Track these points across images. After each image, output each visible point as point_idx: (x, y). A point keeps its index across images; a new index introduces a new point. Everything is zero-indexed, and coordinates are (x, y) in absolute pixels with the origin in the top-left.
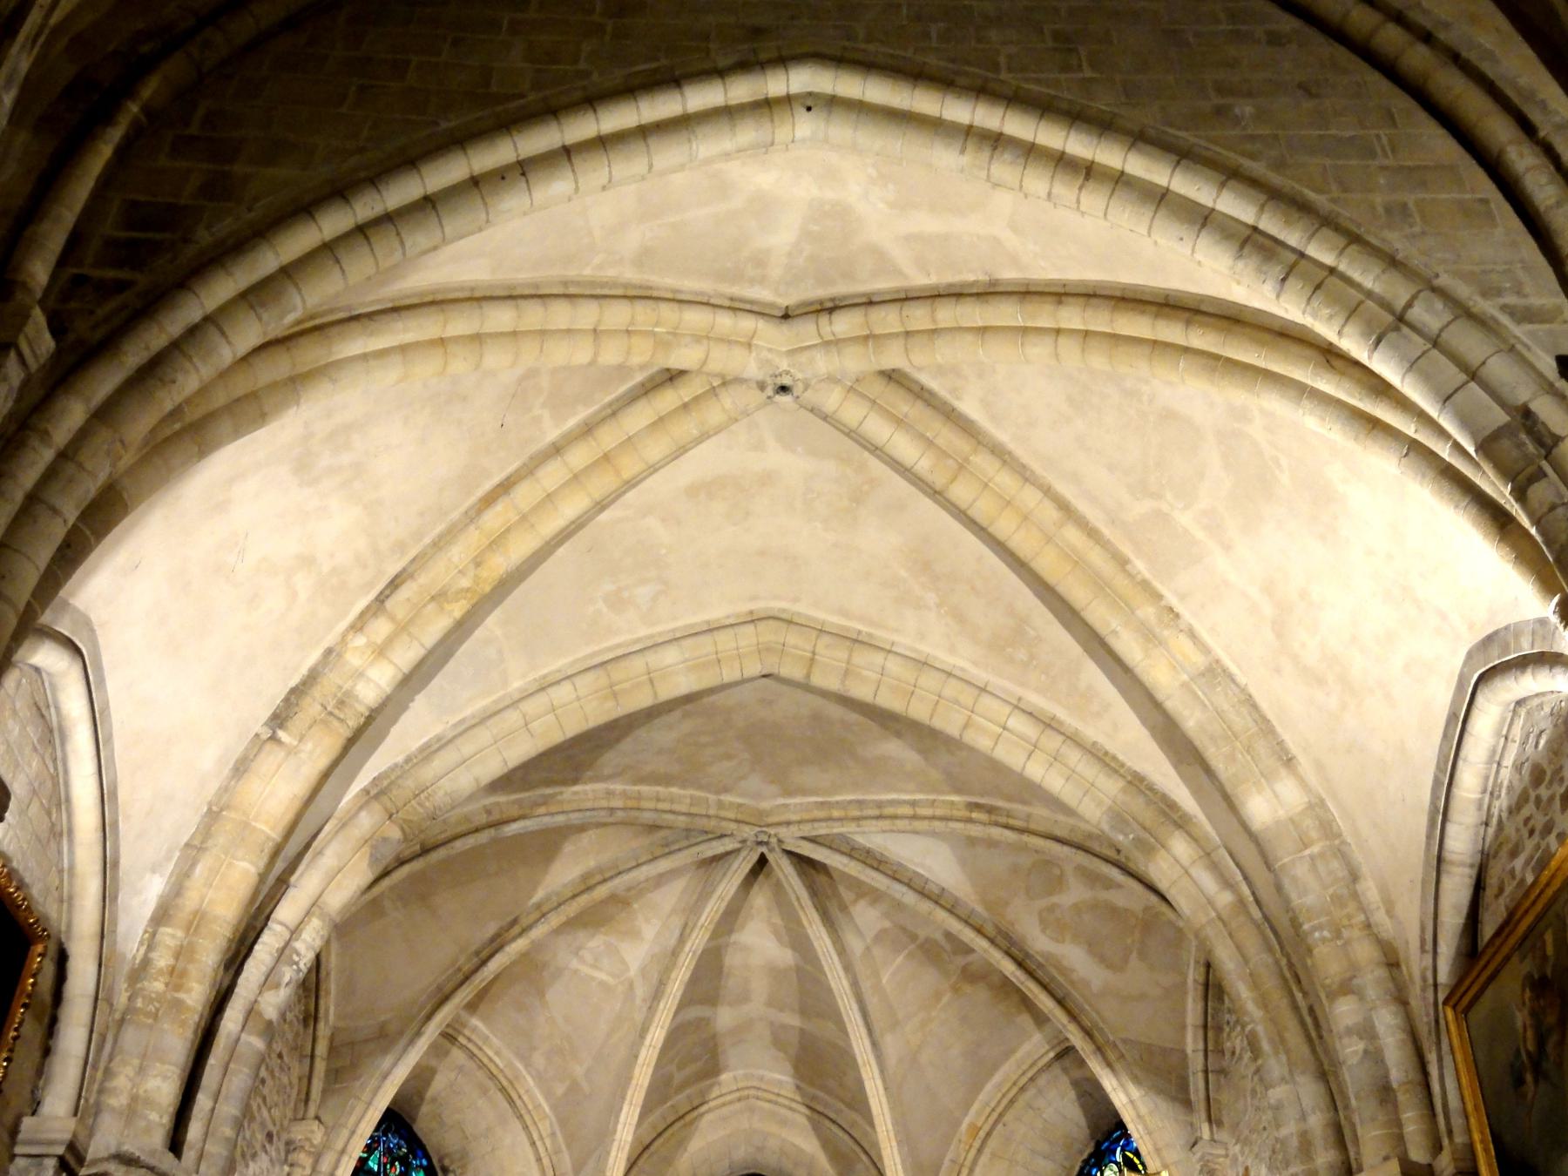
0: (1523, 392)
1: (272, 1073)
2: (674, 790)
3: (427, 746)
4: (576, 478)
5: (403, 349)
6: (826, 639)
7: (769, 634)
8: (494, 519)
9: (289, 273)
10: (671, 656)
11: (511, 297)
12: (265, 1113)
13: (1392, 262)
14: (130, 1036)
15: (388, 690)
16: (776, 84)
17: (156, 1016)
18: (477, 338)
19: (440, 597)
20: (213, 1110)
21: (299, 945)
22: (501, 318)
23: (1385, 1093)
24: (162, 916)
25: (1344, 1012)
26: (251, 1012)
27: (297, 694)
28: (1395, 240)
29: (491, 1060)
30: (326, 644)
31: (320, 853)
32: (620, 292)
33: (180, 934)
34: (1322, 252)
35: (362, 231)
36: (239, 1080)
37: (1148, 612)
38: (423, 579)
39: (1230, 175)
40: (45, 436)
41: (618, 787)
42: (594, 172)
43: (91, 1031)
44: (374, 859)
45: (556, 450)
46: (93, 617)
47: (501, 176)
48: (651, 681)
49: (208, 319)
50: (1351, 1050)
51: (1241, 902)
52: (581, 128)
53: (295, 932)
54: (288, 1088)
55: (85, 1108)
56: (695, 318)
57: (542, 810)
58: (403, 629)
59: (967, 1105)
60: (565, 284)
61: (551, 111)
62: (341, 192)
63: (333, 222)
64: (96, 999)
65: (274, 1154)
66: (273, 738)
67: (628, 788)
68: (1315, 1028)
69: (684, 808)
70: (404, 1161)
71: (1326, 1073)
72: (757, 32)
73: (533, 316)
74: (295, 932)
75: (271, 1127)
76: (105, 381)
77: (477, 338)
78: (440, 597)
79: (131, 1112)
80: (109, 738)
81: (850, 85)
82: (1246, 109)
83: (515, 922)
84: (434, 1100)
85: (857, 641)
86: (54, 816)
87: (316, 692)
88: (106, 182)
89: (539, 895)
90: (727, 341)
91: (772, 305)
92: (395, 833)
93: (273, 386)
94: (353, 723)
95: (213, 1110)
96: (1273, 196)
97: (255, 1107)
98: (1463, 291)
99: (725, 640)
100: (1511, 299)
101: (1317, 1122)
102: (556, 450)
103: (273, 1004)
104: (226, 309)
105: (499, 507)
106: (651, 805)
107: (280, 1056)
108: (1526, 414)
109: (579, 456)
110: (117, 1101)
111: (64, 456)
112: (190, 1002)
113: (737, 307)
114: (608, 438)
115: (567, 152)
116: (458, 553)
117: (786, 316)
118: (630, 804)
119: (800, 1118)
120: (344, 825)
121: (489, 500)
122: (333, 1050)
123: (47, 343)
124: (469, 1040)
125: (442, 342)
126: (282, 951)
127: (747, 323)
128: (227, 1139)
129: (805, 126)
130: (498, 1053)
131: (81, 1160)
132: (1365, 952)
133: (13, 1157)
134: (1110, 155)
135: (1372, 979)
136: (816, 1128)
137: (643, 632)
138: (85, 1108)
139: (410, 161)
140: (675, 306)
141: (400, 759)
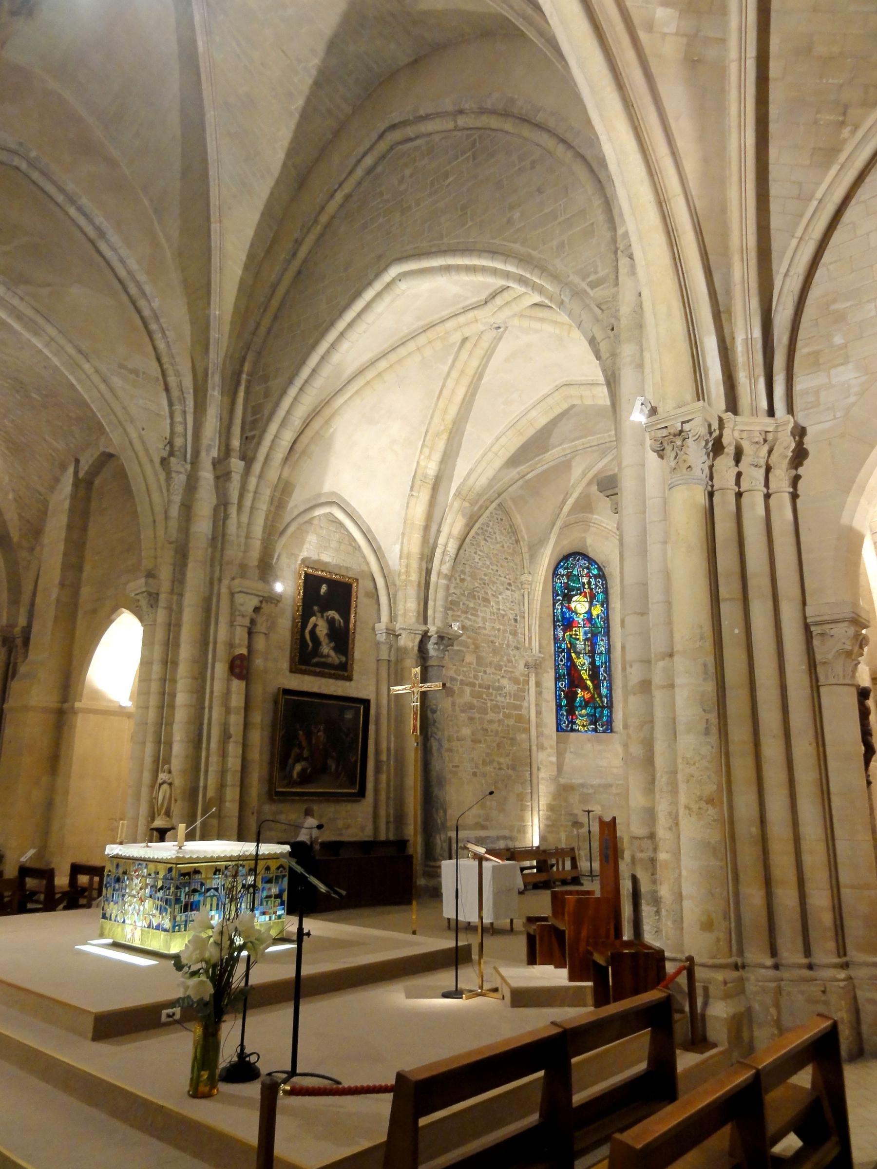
1: (502, 566)
2: (589, 438)
3: (468, 473)
4: (457, 381)
5: (357, 392)
6: (582, 387)
8: (441, 404)
9: (288, 412)
10: (533, 413)
11: (384, 355)
12: (503, 579)
13: (555, 277)
14: (400, 595)
15: (437, 469)
17: (406, 586)
18: (379, 375)
19: (438, 435)
20: (435, 605)
21: (448, 549)
22: (383, 365)
24: (401, 557)
26: (439, 573)
27: (414, 477)
28: (558, 265)
29: (605, 528)
30: (416, 461)
31: (446, 519)
32: (421, 331)
33: (406, 561)
35: (301, 389)
36: (441, 594)
38: (430, 431)
39: (506, 255)
40: (248, 491)
41: (565, 446)
42: (353, 335)
43: (389, 595)
44: (464, 516)
45: (448, 374)
46: (335, 491)
47: (328, 352)
48: (531, 424)
49: (276, 436)
52: (341, 325)
53: (446, 545)
54: (515, 567)
55: (392, 617)
56: (450, 324)
57: (539, 465)
58: (432, 449)
60: (401, 339)
61: (332, 324)
62: (290, 382)
63: (293, 391)
64: (387, 586)
65: (513, 588)
66: (412, 495)
67: (570, 445)
69: (595, 443)
70: (588, 568)
72: (380, 257)
73: (393, 357)
74: (446, 545)
75: (509, 581)
76: (257, 467)
77: (379, 375)
78: (438, 435)
79: (405, 615)
80: (360, 516)
82: (517, 215)
83: (567, 493)
84: (590, 546)
86: (354, 544)
87: (417, 477)
88: (246, 400)
89: (572, 482)
90: (467, 324)
91: (478, 301)
92: (467, 504)
93: (321, 428)
94: (431, 482)
95: (435, 605)
96: (523, 260)
97: (495, 580)
98: (575, 279)
99: (550, 400)
100: (592, 278)
102: (448, 374)
103: (446, 569)
104: (278, 431)
105: (441, 400)
106: (582, 447)
107: (506, 559)
109: (454, 374)
110: (400, 612)
111: (256, 492)
112: (413, 579)
113: (466, 310)
114: (459, 365)
115: (342, 334)
116: (436, 420)
117: (486, 302)
118: (573, 450)
120: (451, 506)
121: (438, 398)
122: (530, 549)
123: (242, 464)
124: (594, 523)
125: (368, 383)
126: (444, 552)
127: (471, 315)
128: (441, 612)
129: (403, 286)
130: (607, 524)
131: (394, 631)
133: (376, 635)
137: (523, 408)
138: (392, 617)
139: (303, 362)
140: (441, 325)
141: (462, 480)
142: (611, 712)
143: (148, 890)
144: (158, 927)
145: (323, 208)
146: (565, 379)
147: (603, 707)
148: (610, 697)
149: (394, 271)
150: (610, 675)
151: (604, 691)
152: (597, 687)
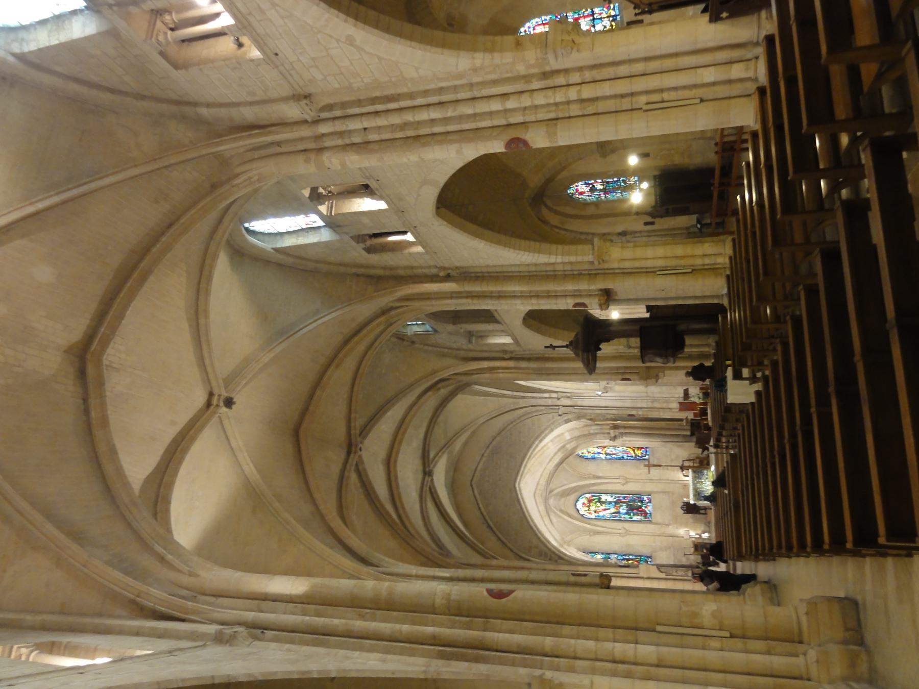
0: (562, 420)
7: (536, 495)
13: (546, 429)
16: (518, 489)
23: (601, 429)
25: (592, 432)
26: (591, 558)
34: (543, 435)
37: (545, 448)
39: (533, 443)
50: (596, 431)
51: (575, 440)
59: (569, 471)
62: (536, 535)
68: (592, 434)
71: (597, 434)
74: (581, 555)
76: (561, 555)
81: (518, 480)
85: (538, 484)
96: (537, 438)
98: (550, 423)
99: (538, 501)
101: (602, 435)
108: (565, 420)
119: (568, 497)
132: (585, 428)
134: (529, 454)
135: (589, 428)
136: (571, 494)
142: (643, 556)
143: (700, 481)
144: (707, 475)
145: (482, 513)
146: (532, 494)
147: (641, 558)
148: (636, 556)
149: (517, 486)
150: (627, 555)
151: (633, 557)
152: (632, 560)
